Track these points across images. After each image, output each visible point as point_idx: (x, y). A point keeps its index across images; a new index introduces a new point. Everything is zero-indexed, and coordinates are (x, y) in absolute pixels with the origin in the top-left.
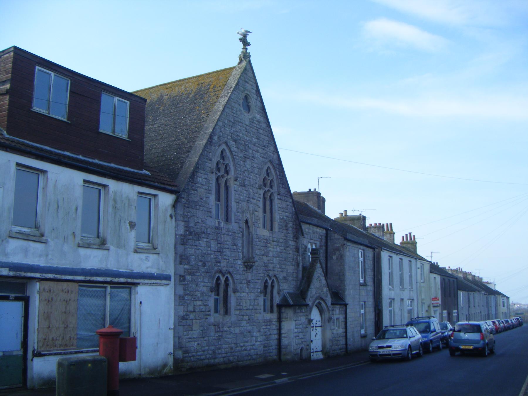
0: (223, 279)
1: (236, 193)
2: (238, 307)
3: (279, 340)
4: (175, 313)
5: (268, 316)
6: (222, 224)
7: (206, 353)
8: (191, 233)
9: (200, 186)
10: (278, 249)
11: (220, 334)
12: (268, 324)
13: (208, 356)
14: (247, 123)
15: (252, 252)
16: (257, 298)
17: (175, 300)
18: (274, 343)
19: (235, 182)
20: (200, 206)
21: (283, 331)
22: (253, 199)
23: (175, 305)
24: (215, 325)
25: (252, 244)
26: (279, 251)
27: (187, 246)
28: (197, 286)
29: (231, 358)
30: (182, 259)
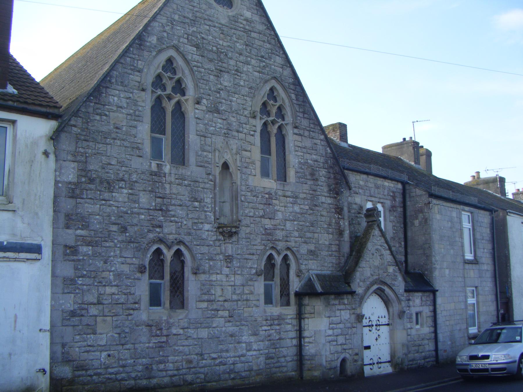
0: (168, 254)
1: (199, 121)
2: (206, 297)
3: (300, 347)
4: (52, 306)
5: (275, 310)
6: (167, 168)
7: (128, 369)
8: (91, 181)
9: (115, 109)
10: (297, 208)
11: (164, 339)
12: (276, 322)
13: (133, 375)
14: (223, 22)
15: (237, 212)
16: (250, 283)
17: (53, 285)
18: (288, 350)
19: (197, 106)
20: (115, 139)
21: (306, 334)
22: (238, 131)
23: (53, 293)
24: (149, 326)
25: (237, 199)
26: (298, 211)
27: (83, 201)
28: (105, 262)
29: (189, 378)
30: (66, 218)
